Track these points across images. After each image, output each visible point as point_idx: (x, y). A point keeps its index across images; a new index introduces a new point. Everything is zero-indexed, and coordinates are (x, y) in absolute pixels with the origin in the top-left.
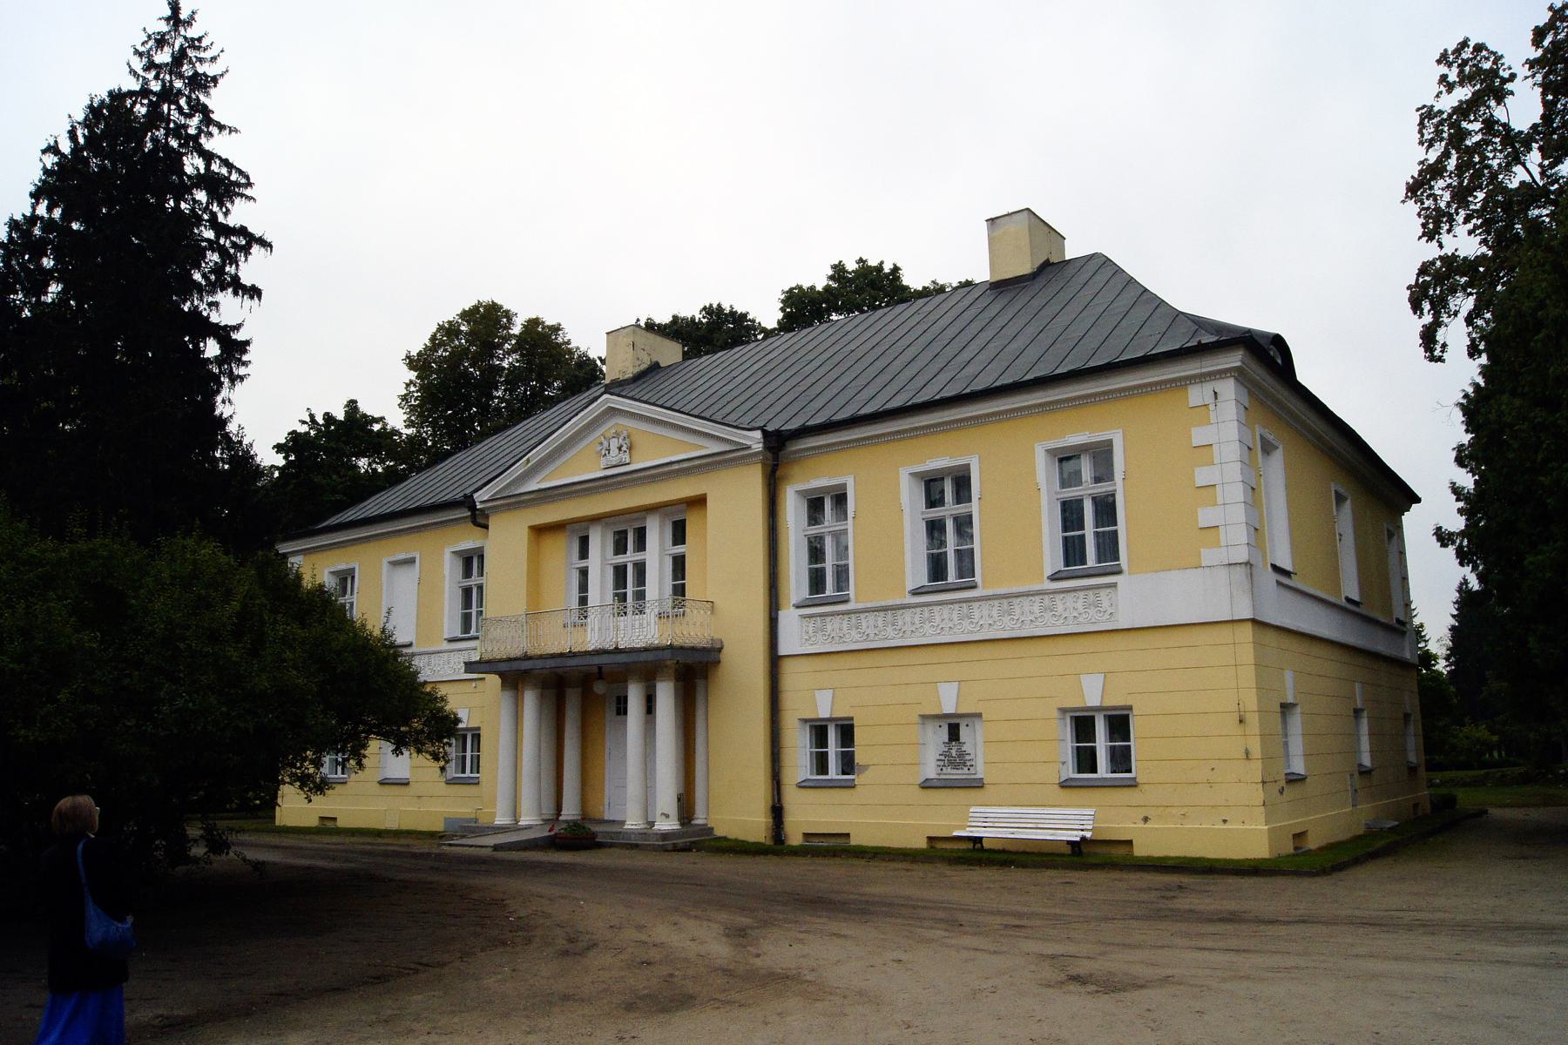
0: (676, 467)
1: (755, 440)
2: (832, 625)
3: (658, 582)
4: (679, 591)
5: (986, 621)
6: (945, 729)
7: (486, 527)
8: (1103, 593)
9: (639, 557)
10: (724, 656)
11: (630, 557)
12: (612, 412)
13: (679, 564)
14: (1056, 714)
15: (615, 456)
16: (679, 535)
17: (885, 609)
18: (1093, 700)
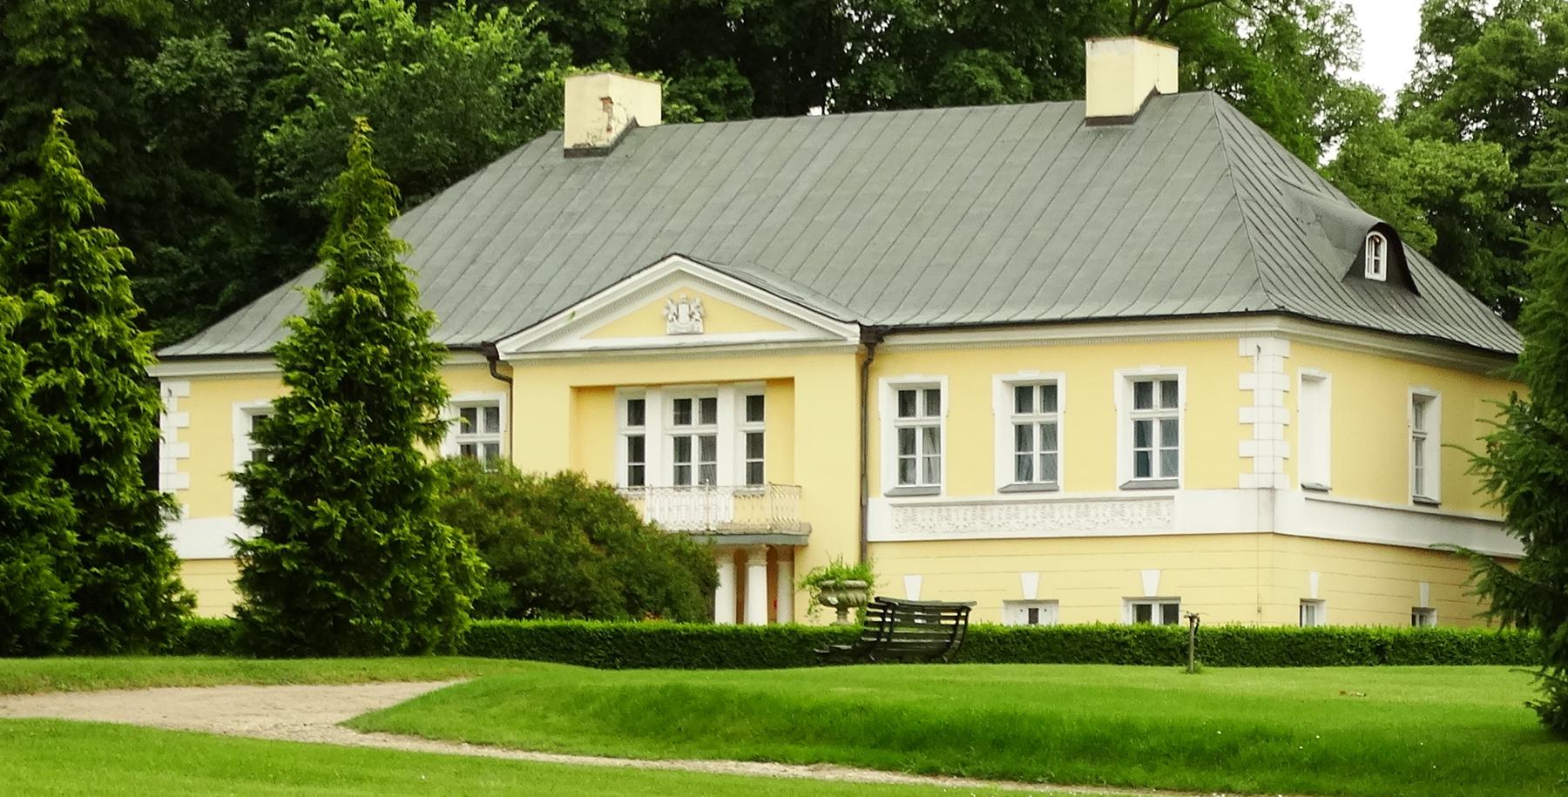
0: (763, 347)
1: (853, 335)
2: (923, 515)
3: (731, 460)
4: (755, 474)
5: (1063, 521)
6: (1027, 613)
7: (510, 381)
8: (1163, 503)
9: (708, 429)
10: (812, 540)
11: (695, 429)
12: (682, 274)
13: (755, 443)
14: (1122, 602)
15: (684, 322)
16: (755, 407)
17: (974, 504)
18: (1150, 592)
